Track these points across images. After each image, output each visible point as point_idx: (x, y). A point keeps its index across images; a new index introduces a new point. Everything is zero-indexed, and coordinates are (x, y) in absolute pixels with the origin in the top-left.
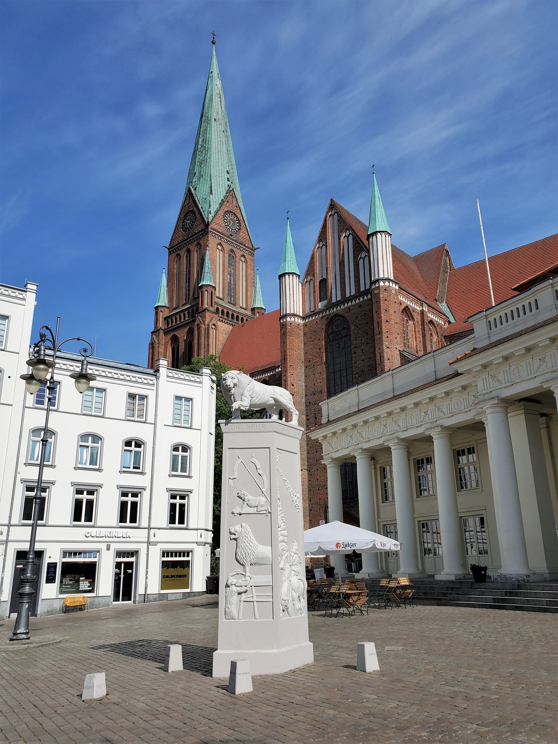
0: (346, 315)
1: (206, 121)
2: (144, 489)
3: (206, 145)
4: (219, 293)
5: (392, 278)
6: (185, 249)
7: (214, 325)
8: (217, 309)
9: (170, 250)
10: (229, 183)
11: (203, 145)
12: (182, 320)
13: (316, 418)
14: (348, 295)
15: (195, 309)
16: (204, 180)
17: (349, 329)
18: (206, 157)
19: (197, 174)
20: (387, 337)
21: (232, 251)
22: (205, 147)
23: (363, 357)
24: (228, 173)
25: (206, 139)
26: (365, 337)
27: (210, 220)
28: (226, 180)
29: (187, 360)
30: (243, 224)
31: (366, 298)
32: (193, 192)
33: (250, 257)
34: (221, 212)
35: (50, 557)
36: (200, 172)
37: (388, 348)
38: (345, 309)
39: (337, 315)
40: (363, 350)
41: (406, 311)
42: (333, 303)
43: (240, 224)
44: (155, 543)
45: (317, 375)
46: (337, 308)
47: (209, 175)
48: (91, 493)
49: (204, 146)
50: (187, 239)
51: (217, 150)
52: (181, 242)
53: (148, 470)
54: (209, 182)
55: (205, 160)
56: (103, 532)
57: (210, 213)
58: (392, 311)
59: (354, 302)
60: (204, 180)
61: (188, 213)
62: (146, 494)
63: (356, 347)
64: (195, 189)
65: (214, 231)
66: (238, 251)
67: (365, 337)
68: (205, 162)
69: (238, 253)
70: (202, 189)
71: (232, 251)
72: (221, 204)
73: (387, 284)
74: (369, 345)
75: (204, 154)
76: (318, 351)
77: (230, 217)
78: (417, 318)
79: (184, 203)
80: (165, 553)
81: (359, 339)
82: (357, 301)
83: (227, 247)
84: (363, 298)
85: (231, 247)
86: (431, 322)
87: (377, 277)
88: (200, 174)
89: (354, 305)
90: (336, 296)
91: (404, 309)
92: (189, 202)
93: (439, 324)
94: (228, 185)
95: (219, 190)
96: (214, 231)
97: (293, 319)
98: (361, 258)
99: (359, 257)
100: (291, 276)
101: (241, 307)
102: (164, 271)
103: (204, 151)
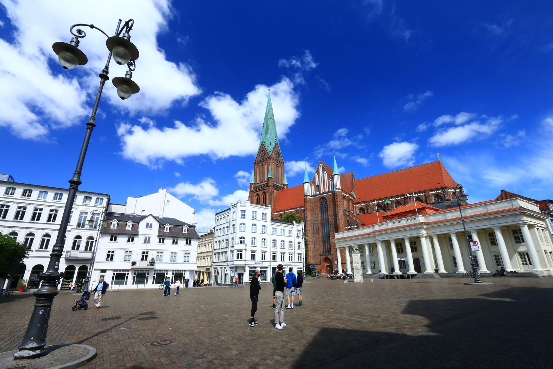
0: (326, 197)
2: (293, 253)
4: (273, 180)
5: (340, 188)
7: (273, 191)
8: (273, 185)
17: (327, 201)
21: (277, 164)
24: (275, 137)
27: (270, 154)
29: (263, 203)
30: (280, 155)
32: (264, 144)
34: (274, 151)
39: (322, 197)
41: (344, 197)
43: (279, 154)
44: (296, 266)
45: (317, 215)
48: (275, 254)
53: (294, 249)
54: (269, 141)
56: (287, 263)
58: (341, 199)
62: (294, 254)
64: (265, 143)
69: (279, 165)
71: (277, 164)
72: (274, 148)
73: (339, 190)
77: (277, 152)
78: (347, 198)
80: (298, 268)
83: (276, 163)
85: (277, 163)
86: (350, 199)
90: (322, 191)
93: (352, 199)
97: (308, 197)
101: (280, 184)
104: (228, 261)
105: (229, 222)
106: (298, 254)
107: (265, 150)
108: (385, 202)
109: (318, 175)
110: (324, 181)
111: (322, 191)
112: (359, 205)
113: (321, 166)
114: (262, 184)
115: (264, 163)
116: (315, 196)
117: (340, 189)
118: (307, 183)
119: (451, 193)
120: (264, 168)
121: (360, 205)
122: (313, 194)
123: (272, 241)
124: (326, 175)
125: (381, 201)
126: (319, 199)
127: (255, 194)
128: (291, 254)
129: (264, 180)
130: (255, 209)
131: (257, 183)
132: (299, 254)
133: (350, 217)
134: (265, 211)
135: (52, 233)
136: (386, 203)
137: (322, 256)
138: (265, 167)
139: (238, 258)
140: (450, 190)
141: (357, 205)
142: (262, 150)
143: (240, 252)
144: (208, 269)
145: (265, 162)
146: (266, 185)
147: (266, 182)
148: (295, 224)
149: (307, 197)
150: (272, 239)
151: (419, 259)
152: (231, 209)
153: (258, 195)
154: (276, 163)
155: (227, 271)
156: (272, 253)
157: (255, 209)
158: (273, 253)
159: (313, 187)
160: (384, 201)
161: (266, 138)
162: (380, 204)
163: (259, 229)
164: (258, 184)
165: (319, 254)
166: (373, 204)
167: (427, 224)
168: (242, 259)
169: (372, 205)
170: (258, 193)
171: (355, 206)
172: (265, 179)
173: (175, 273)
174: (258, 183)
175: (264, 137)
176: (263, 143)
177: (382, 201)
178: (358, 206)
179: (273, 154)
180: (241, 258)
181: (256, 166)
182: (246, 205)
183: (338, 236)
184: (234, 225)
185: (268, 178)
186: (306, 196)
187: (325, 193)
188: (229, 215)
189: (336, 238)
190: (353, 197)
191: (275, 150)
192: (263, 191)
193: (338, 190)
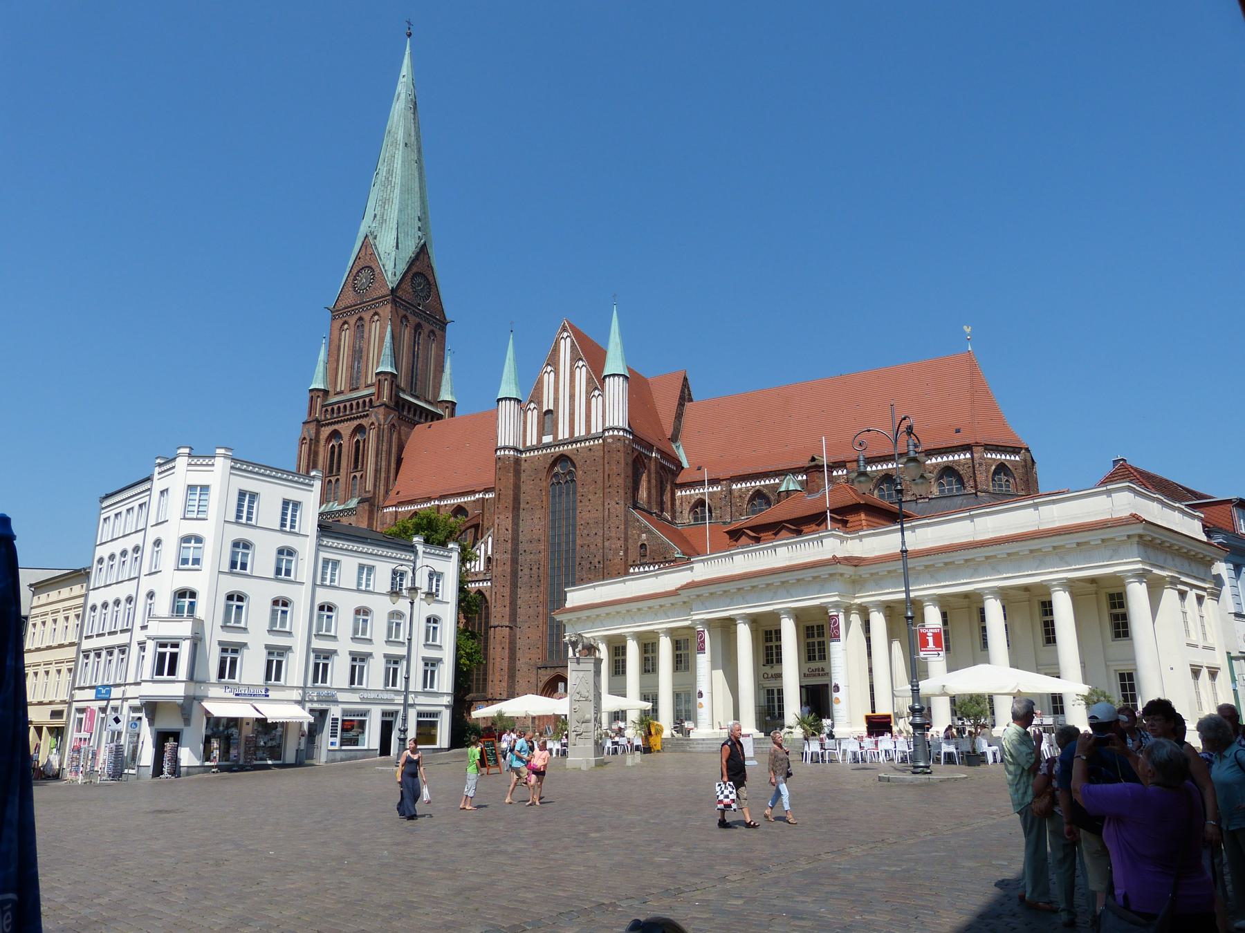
0: (573, 457)
1: (394, 144)
3: (392, 178)
5: (627, 427)
6: (356, 317)
9: (334, 314)
10: (420, 234)
11: (388, 178)
12: (348, 413)
13: (531, 569)
14: (577, 434)
15: (367, 400)
16: (387, 228)
18: (391, 195)
19: (378, 217)
20: (618, 492)
22: (391, 181)
23: (590, 507)
24: (419, 220)
25: (393, 171)
26: (593, 486)
28: (417, 229)
31: (596, 442)
33: (441, 332)
34: (410, 275)
35: (333, 715)
36: (383, 215)
37: (617, 503)
38: (572, 450)
40: (589, 500)
42: (559, 441)
44: (412, 705)
45: (536, 521)
46: (563, 447)
47: (395, 222)
49: (390, 179)
50: (361, 304)
51: (407, 187)
52: (351, 307)
55: (391, 200)
57: (395, 275)
59: (583, 444)
60: (387, 228)
61: (363, 268)
63: (582, 496)
64: (375, 238)
65: (398, 300)
66: (427, 325)
67: (593, 486)
68: (390, 203)
70: (385, 238)
74: (597, 495)
75: (389, 191)
76: (539, 492)
77: (419, 280)
79: (358, 254)
80: (420, 714)
81: (587, 487)
82: (587, 444)
83: (413, 320)
84: (594, 442)
87: (611, 425)
88: (383, 217)
89: (583, 448)
90: (563, 433)
91: (637, 457)
92: (366, 254)
94: (419, 237)
95: (407, 243)
96: (398, 300)
98: (594, 396)
99: (592, 394)
100: (512, 402)
102: (324, 342)
103: (390, 186)
104: (126, 685)
105: (145, 529)
106: (422, 664)
107: (373, 267)
108: (779, 485)
109: (552, 374)
110: (572, 397)
111: (563, 433)
112: (693, 492)
113: (565, 339)
114: (355, 395)
115: (367, 316)
116: (538, 449)
117: (624, 430)
118: (510, 399)
119: (993, 467)
120: (366, 336)
121: (697, 491)
122: (528, 444)
123: (316, 609)
124: (582, 375)
125: (767, 482)
126: (550, 461)
127: (326, 432)
128: (393, 660)
129: (363, 381)
130: (250, 485)
131: (338, 390)
132: (431, 664)
133: (649, 532)
134: (294, 494)
136: (783, 489)
137: (542, 671)
138: (370, 332)
139: (160, 672)
140: (989, 456)
141: (688, 492)
142: (361, 264)
143: (169, 650)
144: (56, 714)
145: (372, 312)
146: (371, 400)
147: (372, 390)
148: (420, 548)
149: (507, 452)
150: (318, 602)
151: (827, 685)
152: (156, 476)
153: (335, 434)
154: (413, 320)
155: (117, 720)
156: (312, 656)
157: (250, 485)
158: (317, 657)
159: (533, 417)
160: (777, 481)
161: (383, 221)
162: (765, 491)
163: (263, 560)
164: (338, 393)
165: (532, 662)
166: (741, 489)
167: (855, 562)
168: (174, 674)
169: (736, 494)
170: (336, 427)
171: (679, 493)
172: (366, 377)
174: (341, 392)
175: (375, 216)
176: (370, 238)
177: (772, 482)
178: (691, 495)
179: (407, 286)
180: (172, 671)
181: (339, 322)
182: (213, 465)
183: (576, 597)
185: (378, 374)
186: (505, 448)
187: (572, 443)
188: (145, 503)
189: (568, 605)
190: (673, 463)
191: (414, 269)
192: (356, 423)
193: (616, 433)
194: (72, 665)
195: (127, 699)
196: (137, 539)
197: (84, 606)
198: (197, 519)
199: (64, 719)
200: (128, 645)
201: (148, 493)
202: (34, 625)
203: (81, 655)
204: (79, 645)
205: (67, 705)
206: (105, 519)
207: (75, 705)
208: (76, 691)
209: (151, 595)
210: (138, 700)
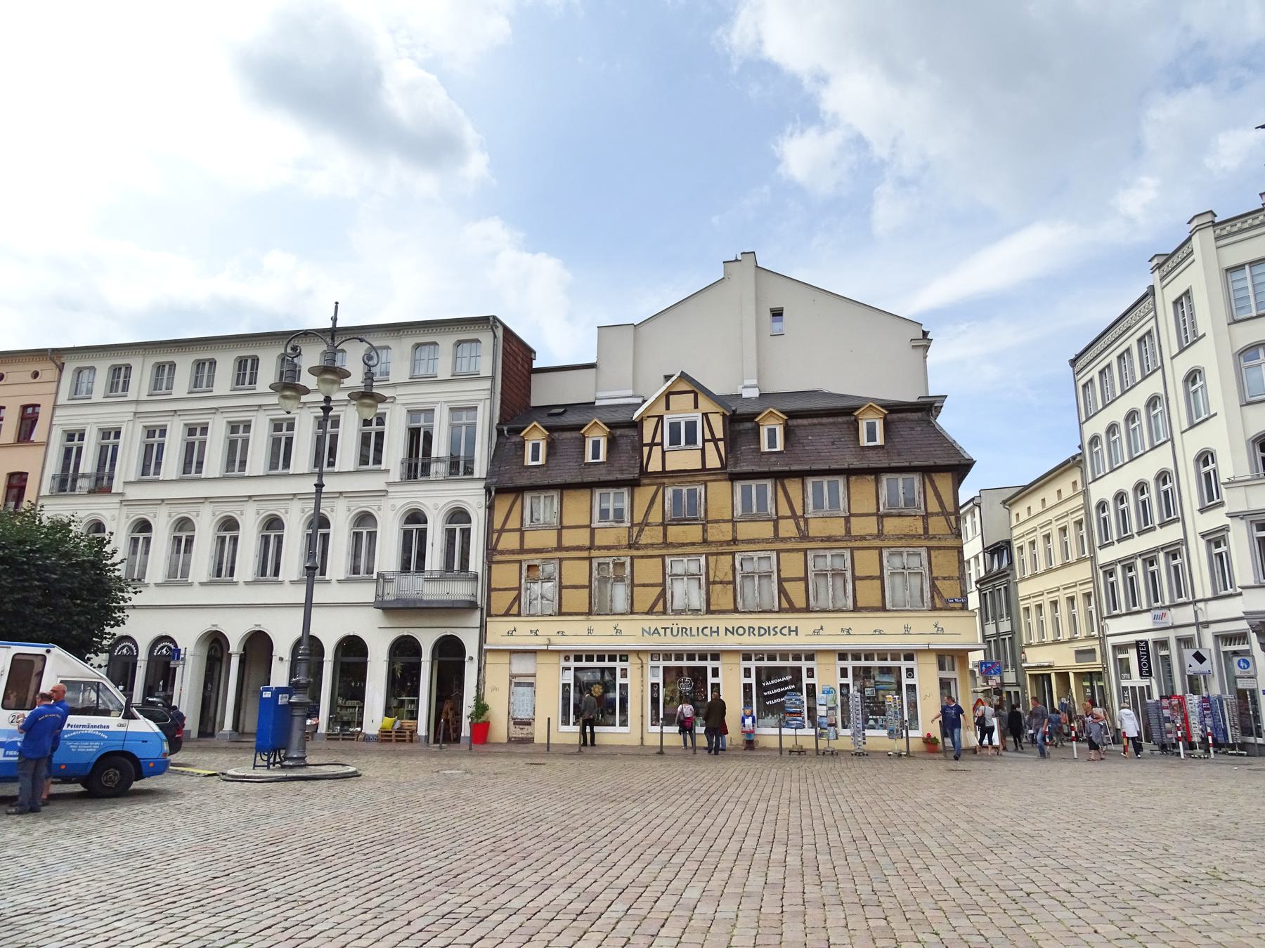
104: (1195, 602)
135: (376, 508)
155: (1200, 658)
173: (854, 668)
184: (1193, 376)
188: (1149, 333)
194: (1089, 588)
195: (1207, 624)
196: (1153, 386)
197: (1086, 505)
198: (1258, 316)
199: (1099, 661)
200: (1184, 541)
201: (1152, 313)
202: (1021, 548)
203: (1101, 572)
204: (1093, 559)
205: (1098, 642)
206: (1085, 386)
207: (1111, 641)
208: (1108, 621)
209: (1205, 457)
210: (1245, 622)
